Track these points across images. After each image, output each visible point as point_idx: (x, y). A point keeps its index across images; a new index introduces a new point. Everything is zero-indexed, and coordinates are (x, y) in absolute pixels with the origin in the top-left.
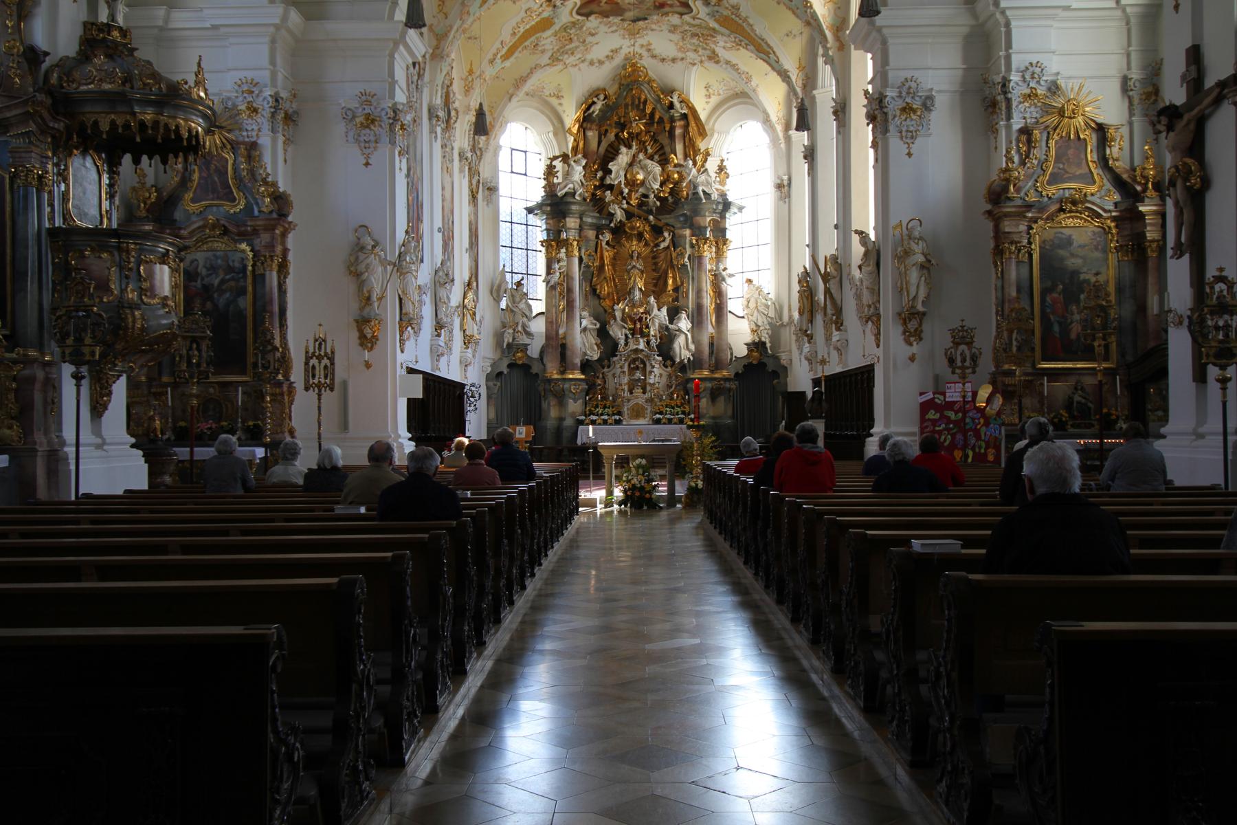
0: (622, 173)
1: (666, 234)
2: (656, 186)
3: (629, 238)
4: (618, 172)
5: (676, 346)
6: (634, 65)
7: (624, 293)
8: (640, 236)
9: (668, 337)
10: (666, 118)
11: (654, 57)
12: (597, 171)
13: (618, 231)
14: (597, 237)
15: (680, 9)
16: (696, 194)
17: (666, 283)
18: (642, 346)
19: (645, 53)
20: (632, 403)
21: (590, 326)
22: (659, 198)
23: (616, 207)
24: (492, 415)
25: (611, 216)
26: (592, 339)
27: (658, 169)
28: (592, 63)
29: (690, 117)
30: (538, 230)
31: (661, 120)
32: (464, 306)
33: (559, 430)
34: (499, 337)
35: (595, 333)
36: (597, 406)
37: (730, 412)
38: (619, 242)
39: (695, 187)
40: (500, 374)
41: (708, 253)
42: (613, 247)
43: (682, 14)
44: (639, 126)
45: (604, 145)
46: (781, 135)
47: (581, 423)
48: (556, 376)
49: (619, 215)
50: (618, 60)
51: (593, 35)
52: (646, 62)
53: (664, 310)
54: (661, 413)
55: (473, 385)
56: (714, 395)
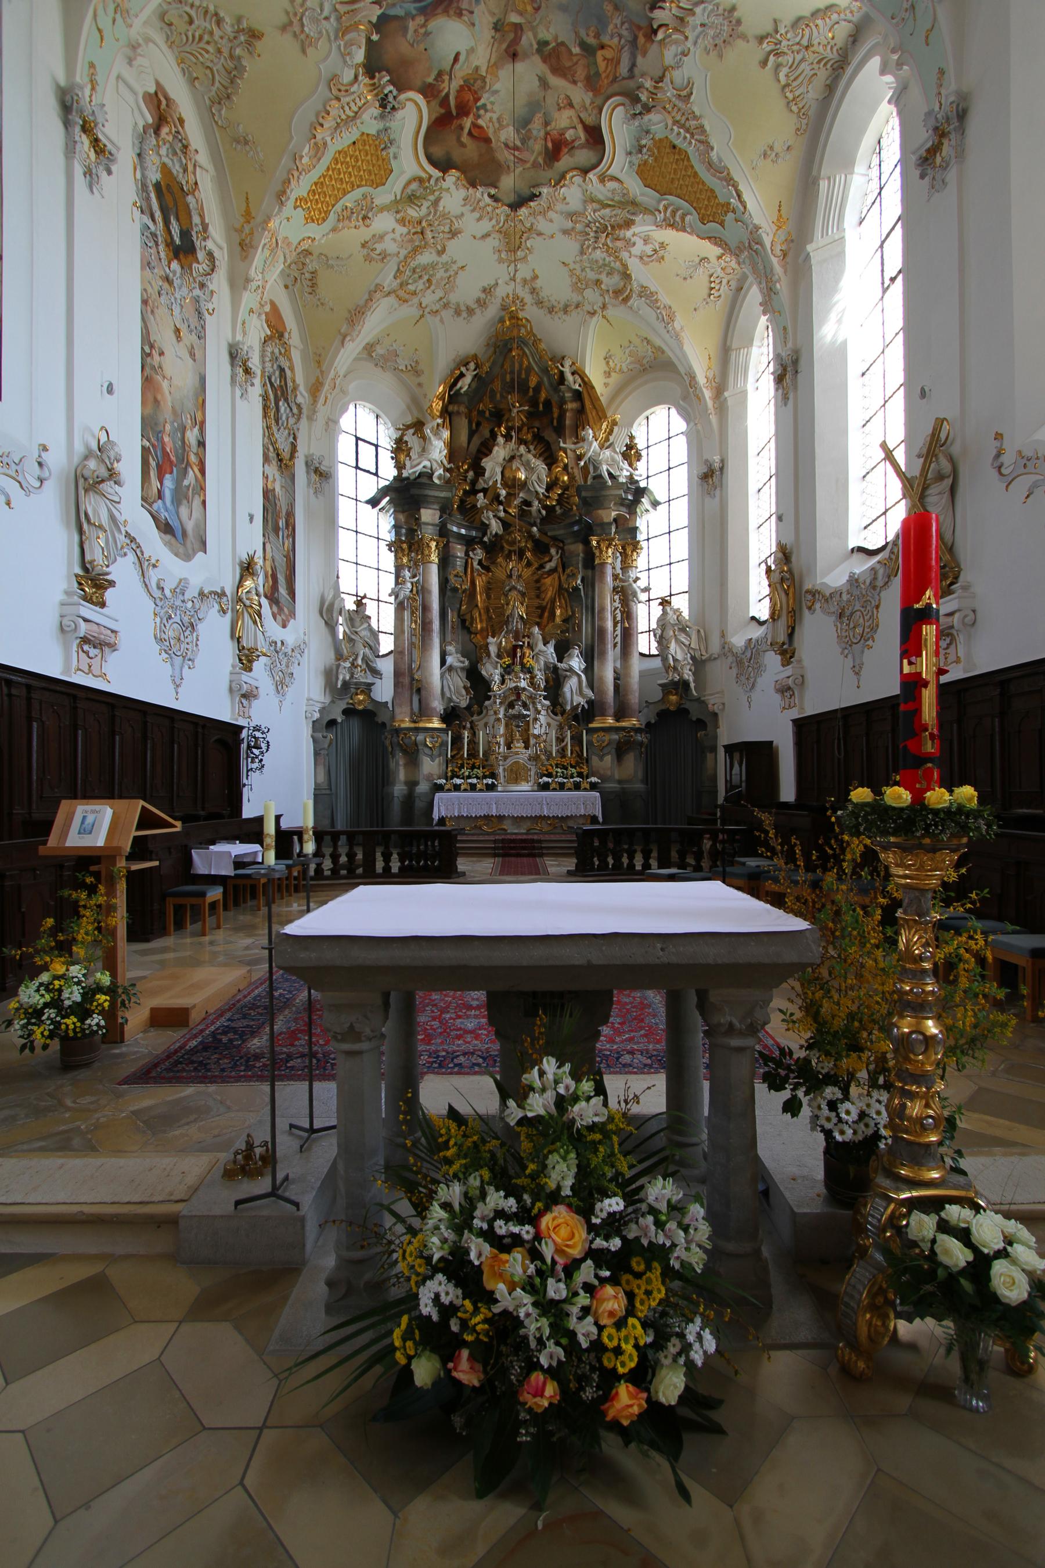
0: (499, 470)
1: (553, 551)
2: (541, 491)
3: (508, 557)
4: (493, 469)
5: (566, 689)
6: (514, 317)
7: (498, 623)
8: (521, 554)
9: (555, 681)
10: (555, 399)
11: (539, 303)
12: (467, 471)
13: (493, 548)
14: (467, 554)
15: (584, 156)
16: (600, 476)
17: (553, 615)
18: (523, 684)
19: (528, 299)
20: (510, 761)
21: (457, 664)
22: (545, 507)
23: (491, 514)
24: (322, 778)
25: (484, 527)
26: (459, 681)
27: (541, 467)
28: (458, 312)
29: (584, 395)
30: (382, 524)
31: (548, 403)
32: (240, 600)
33: (409, 799)
34: (330, 675)
35: (463, 675)
36: (462, 766)
37: (640, 775)
38: (494, 563)
39: (596, 468)
40: (332, 723)
41: (610, 558)
42: (487, 569)
43: (585, 171)
44: (518, 410)
45: (476, 441)
46: (710, 403)
47: (439, 788)
48: (407, 724)
49: (495, 527)
50: (492, 311)
51: (454, 234)
52: (530, 312)
53: (550, 649)
54: (549, 775)
55: (257, 728)
56: (621, 750)
